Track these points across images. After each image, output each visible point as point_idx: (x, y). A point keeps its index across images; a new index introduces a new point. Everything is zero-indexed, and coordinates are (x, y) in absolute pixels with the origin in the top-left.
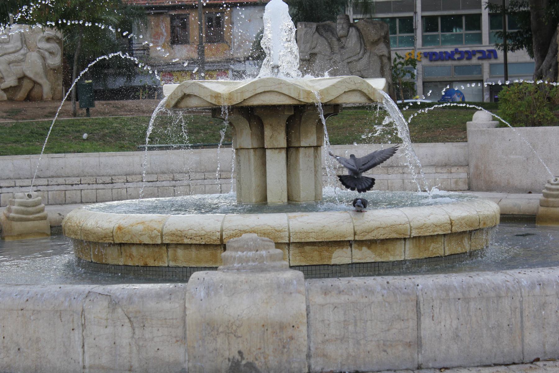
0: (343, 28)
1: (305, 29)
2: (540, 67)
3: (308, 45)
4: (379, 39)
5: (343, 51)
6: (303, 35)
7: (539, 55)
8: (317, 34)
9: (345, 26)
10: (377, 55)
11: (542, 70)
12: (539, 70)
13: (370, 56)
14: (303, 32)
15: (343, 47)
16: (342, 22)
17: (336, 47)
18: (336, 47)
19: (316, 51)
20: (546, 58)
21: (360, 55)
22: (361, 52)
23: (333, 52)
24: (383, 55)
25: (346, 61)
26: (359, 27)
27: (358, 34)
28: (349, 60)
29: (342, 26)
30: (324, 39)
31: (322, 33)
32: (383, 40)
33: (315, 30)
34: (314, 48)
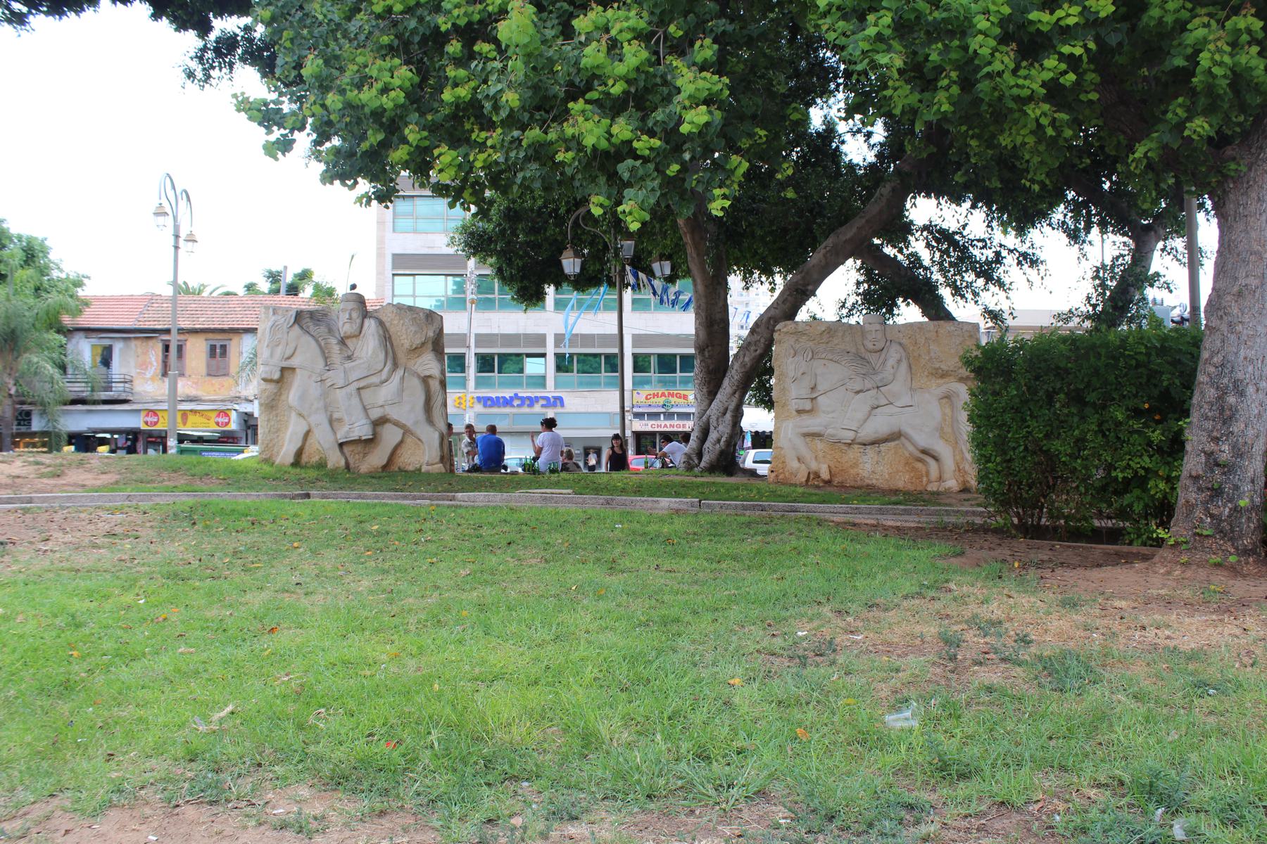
0: (350, 318)
1: (273, 318)
2: (706, 411)
3: (279, 350)
4: (423, 344)
5: (348, 365)
6: (268, 330)
7: (705, 390)
8: (296, 326)
9: (355, 315)
10: (419, 376)
11: (708, 420)
12: (704, 418)
13: (403, 378)
14: (270, 324)
15: (349, 358)
16: (350, 307)
17: (336, 356)
18: (336, 356)
19: (294, 362)
20: (718, 396)
21: (384, 375)
22: (386, 369)
23: (328, 365)
24: (430, 376)
25: (356, 385)
26: (384, 319)
27: (381, 332)
28: (362, 384)
29: (350, 315)
30: (310, 339)
31: (308, 327)
32: (430, 346)
33: (292, 320)
34: (289, 358)
